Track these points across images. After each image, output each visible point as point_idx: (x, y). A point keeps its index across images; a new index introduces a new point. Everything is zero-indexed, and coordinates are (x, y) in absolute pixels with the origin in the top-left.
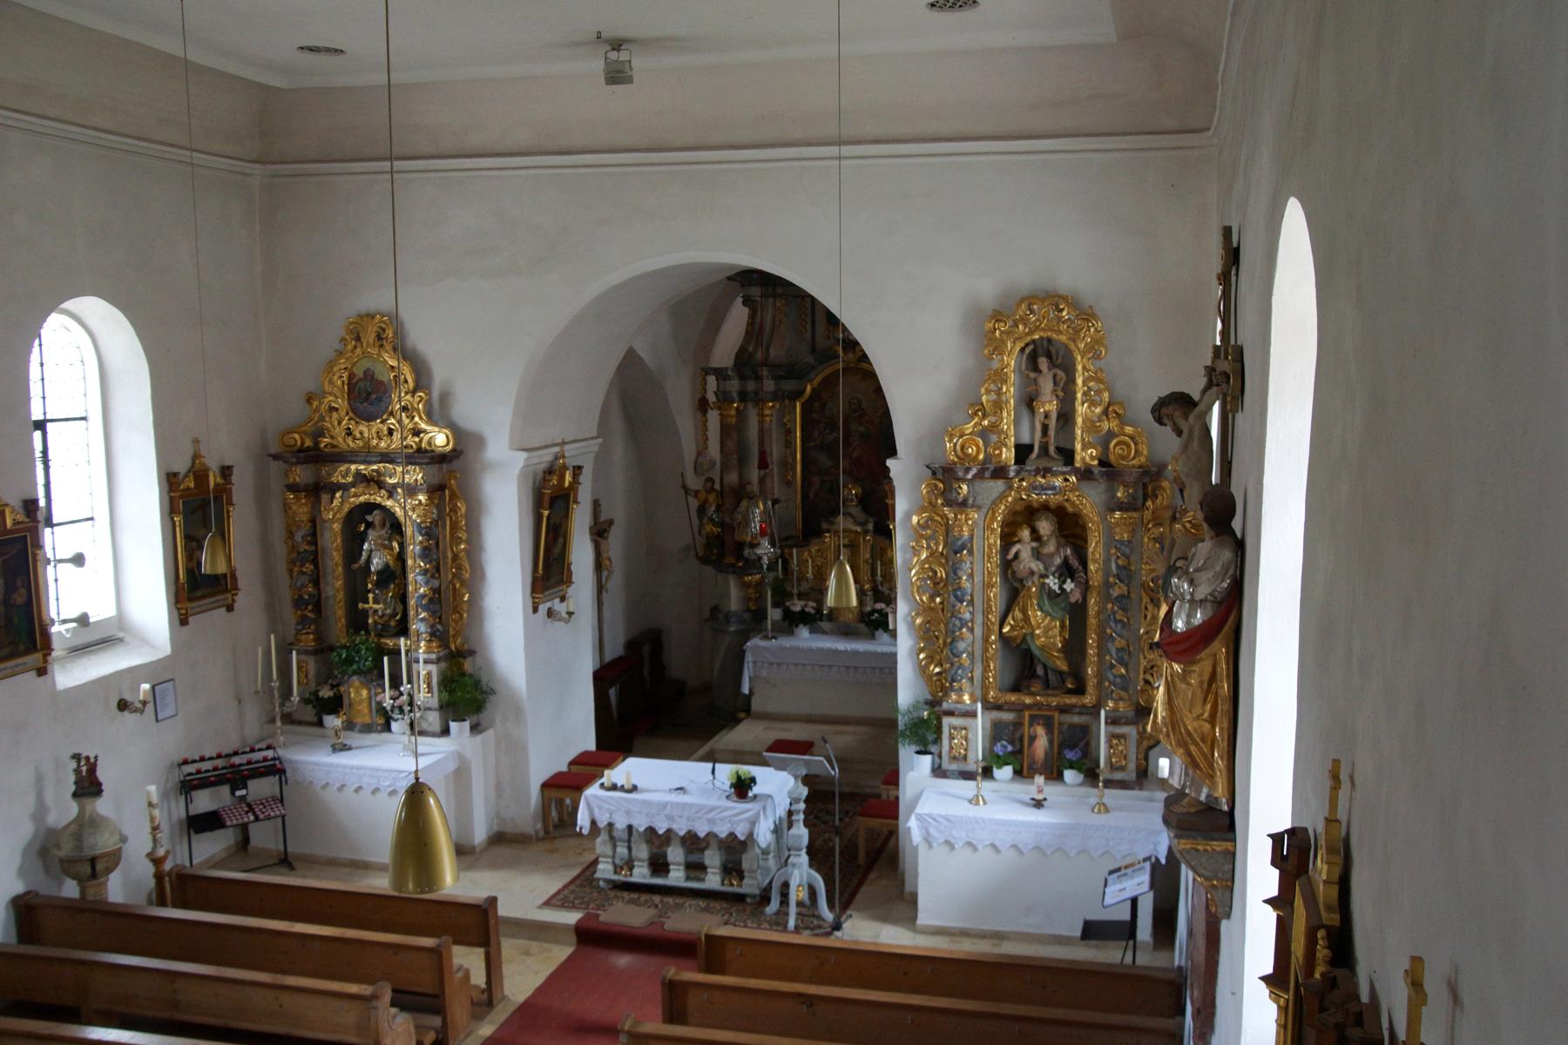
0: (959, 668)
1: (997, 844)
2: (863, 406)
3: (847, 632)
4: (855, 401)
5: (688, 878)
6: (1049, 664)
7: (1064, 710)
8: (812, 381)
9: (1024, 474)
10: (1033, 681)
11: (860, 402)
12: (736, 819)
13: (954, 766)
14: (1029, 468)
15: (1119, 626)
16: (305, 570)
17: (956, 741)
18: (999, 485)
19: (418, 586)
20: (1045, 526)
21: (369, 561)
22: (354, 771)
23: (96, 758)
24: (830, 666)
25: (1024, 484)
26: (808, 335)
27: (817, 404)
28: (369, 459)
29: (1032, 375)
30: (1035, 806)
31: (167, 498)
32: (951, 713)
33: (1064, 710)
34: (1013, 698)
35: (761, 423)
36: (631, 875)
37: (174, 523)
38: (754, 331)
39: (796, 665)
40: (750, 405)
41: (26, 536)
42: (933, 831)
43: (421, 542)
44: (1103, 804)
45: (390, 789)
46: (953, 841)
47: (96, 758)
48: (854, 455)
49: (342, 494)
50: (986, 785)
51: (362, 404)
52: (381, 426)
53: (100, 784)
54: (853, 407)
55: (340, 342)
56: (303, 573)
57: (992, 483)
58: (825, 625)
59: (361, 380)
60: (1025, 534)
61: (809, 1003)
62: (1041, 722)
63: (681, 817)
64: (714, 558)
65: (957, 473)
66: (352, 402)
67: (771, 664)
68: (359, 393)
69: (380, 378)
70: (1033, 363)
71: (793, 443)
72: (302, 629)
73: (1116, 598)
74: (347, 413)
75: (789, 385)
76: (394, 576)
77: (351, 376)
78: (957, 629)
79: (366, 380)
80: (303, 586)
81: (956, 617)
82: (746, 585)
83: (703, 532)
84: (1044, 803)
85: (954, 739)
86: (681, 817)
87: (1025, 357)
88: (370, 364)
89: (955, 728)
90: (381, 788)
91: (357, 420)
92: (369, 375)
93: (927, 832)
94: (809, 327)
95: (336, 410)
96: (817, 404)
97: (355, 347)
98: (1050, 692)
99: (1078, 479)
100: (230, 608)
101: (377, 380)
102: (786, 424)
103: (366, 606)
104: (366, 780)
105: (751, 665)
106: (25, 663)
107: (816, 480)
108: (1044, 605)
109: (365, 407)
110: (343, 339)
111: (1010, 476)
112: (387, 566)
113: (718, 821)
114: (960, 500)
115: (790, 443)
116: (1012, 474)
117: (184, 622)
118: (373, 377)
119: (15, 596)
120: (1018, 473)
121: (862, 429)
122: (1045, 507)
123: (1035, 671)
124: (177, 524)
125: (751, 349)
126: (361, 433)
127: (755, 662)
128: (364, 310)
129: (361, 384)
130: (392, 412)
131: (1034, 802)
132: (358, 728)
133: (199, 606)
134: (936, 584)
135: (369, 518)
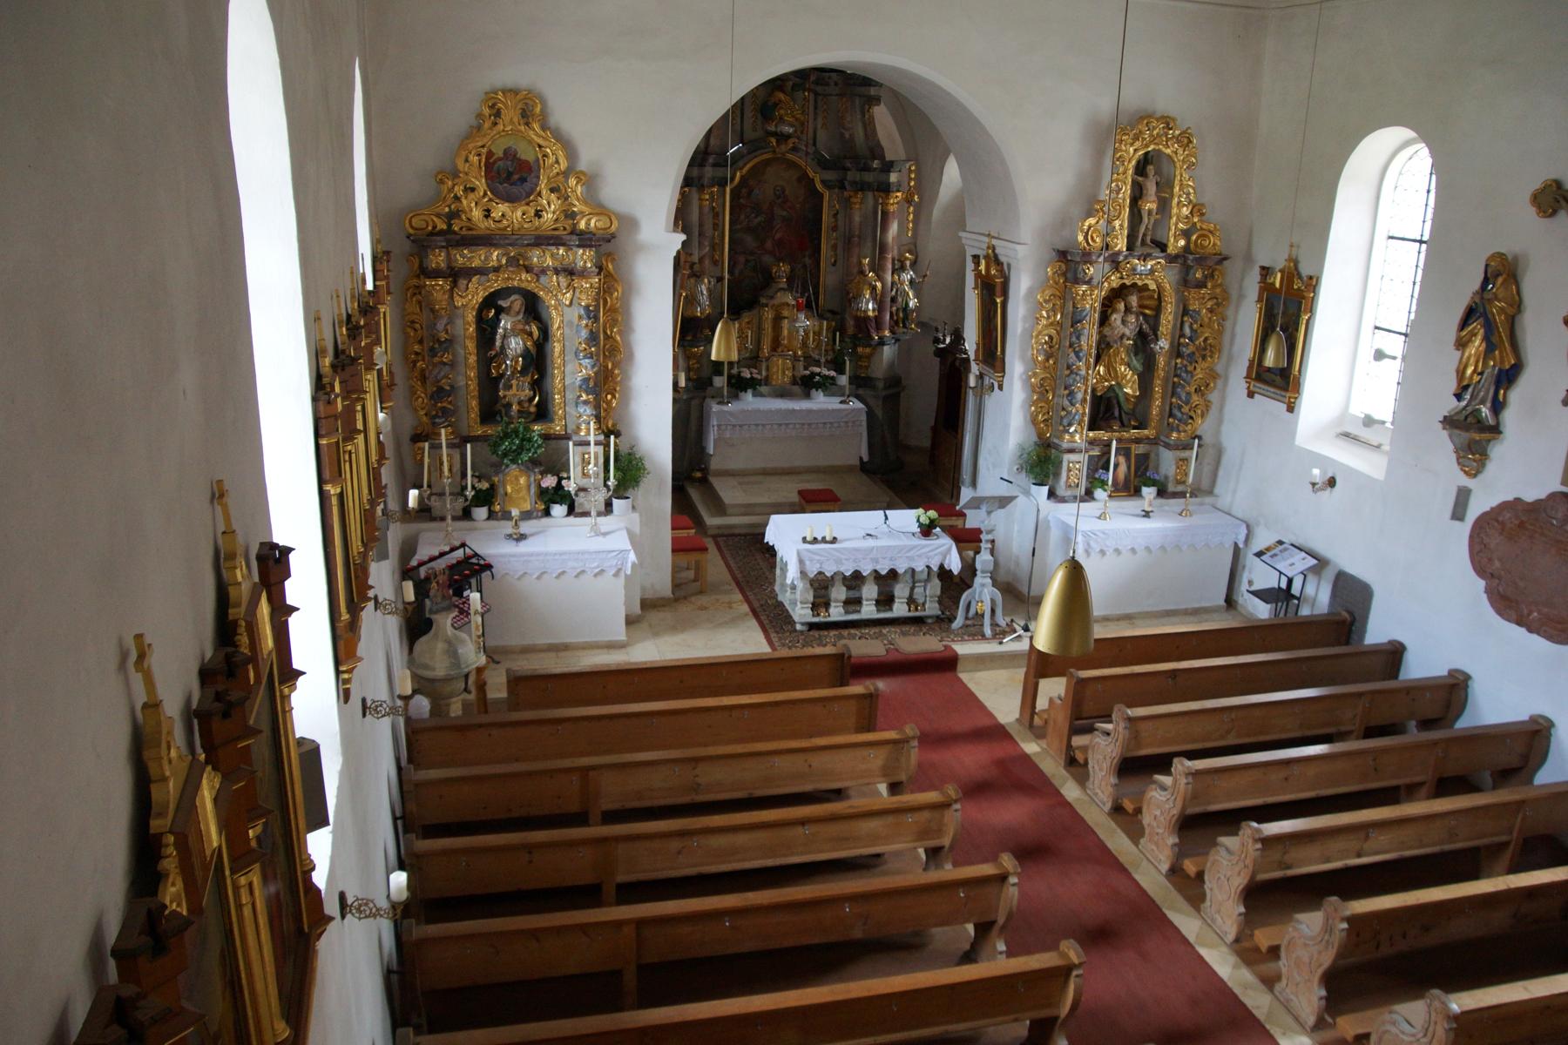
1: (1136, 547)
2: (787, 192)
3: (782, 394)
4: (778, 188)
5: (847, 612)
7: (1138, 441)
8: (741, 169)
10: (1112, 421)
12: (931, 554)
13: (1068, 493)
15: (1189, 375)
16: (445, 360)
21: (503, 347)
22: (556, 557)
24: (787, 424)
25: (1128, 265)
27: (744, 190)
29: (1140, 179)
30: (1144, 516)
32: (1071, 451)
35: (701, 207)
36: (829, 615)
39: (757, 425)
40: (694, 189)
42: (1092, 543)
45: (597, 570)
46: (1105, 549)
48: (778, 236)
49: (479, 279)
51: (501, 184)
52: (525, 208)
56: (445, 364)
58: (763, 389)
59: (500, 159)
60: (1121, 306)
63: (884, 558)
66: (489, 181)
67: (734, 426)
68: (498, 173)
69: (523, 157)
70: (1141, 169)
71: (720, 224)
72: (444, 422)
73: (1189, 355)
76: (537, 361)
77: (490, 154)
81: (1077, 374)
84: (1151, 514)
85: (1070, 471)
86: (884, 558)
88: (512, 143)
90: (587, 570)
92: (509, 154)
93: (1088, 544)
95: (473, 190)
96: (744, 190)
97: (495, 124)
101: (520, 160)
102: (714, 208)
104: (571, 564)
105: (716, 428)
107: (742, 259)
108: (1132, 361)
112: (526, 350)
113: (916, 558)
116: (1121, 258)
118: (515, 156)
120: (1126, 257)
121: (785, 213)
123: (1113, 414)
127: (719, 426)
129: (500, 163)
131: (1144, 513)
133: (1274, 393)
134: (1051, 347)
135: (504, 303)
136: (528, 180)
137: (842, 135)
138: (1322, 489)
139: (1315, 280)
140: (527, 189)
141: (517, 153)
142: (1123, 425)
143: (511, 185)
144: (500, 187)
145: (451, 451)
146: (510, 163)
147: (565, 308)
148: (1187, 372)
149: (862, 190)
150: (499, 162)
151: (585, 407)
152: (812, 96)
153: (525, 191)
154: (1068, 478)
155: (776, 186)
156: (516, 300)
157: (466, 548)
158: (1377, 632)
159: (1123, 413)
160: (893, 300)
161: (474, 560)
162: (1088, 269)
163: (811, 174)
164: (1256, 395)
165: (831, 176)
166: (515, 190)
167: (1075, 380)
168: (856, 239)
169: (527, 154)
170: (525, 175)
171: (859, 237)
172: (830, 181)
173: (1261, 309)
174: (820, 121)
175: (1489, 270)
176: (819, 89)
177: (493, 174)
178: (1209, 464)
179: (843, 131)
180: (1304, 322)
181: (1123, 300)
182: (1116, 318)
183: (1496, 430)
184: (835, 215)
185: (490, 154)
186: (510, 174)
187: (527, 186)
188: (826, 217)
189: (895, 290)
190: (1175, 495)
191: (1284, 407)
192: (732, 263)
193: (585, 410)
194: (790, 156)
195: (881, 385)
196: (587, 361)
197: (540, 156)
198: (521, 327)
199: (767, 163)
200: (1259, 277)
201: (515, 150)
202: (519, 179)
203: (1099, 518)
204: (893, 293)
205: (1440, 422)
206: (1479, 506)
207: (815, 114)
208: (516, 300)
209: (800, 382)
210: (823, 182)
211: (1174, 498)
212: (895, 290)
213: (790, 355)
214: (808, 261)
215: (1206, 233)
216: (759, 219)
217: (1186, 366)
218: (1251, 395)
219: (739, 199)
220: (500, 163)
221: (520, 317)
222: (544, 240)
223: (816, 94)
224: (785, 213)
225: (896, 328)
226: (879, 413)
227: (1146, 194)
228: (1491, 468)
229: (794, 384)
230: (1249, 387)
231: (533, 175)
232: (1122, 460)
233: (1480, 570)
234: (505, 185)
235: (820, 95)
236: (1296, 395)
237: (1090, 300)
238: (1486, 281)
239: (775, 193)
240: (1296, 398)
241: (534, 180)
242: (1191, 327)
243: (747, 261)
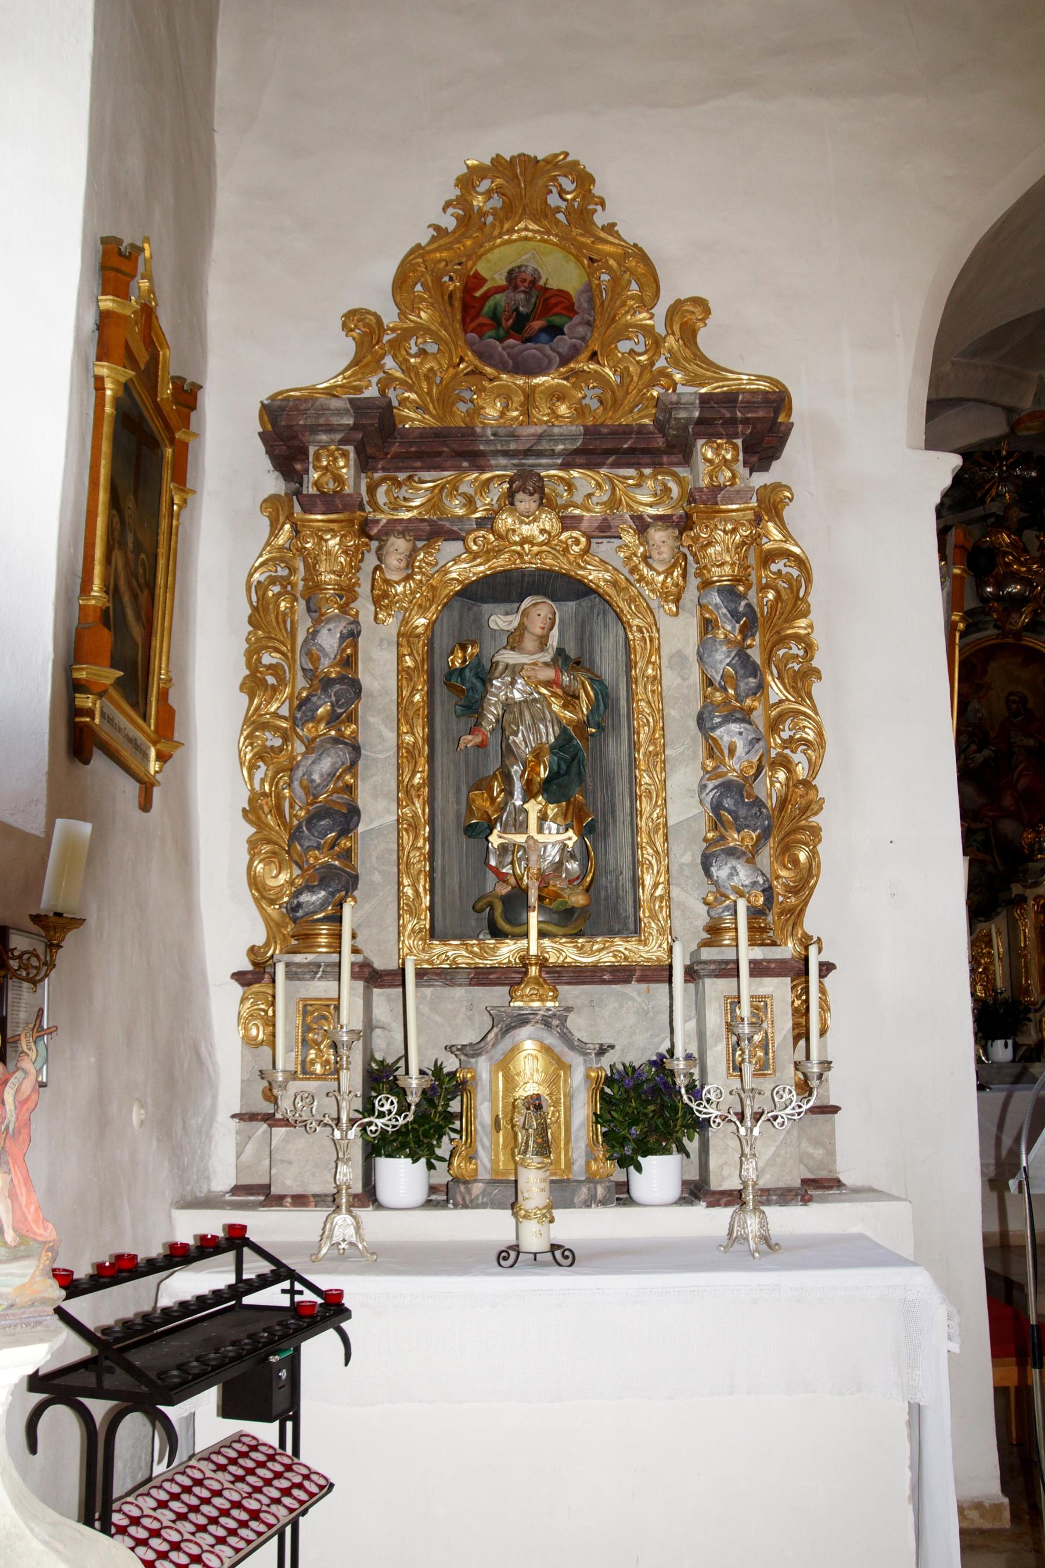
2: (1030, 705)
4: (1016, 698)
11: (1023, 700)
48: (1022, 784)
51: (501, 340)
54: (1014, 706)
55: (444, 210)
59: (499, 290)
69: (553, 285)
79: (515, 288)
91: (489, 370)
101: (545, 289)
109: (513, 347)
110: (448, 205)
118: (534, 282)
121: (1031, 742)
136: (566, 330)
140: (564, 349)
141: (540, 277)
146: (522, 296)
150: (498, 297)
151: (733, 862)
153: (559, 354)
155: (1011, 694)
166: (532, 350)
170: (557, 320)
177: (481, 320)
186: (520, 322)
187: (563, 343)
193: (734, 872)
196: (735, 727)
198: (550, 674)
202: (542, 330)
216: (986, 753)
221: (547, 657)
224: (1031, 742)
231: (577, 319)
234: (511, 341)
241: (581, 330)
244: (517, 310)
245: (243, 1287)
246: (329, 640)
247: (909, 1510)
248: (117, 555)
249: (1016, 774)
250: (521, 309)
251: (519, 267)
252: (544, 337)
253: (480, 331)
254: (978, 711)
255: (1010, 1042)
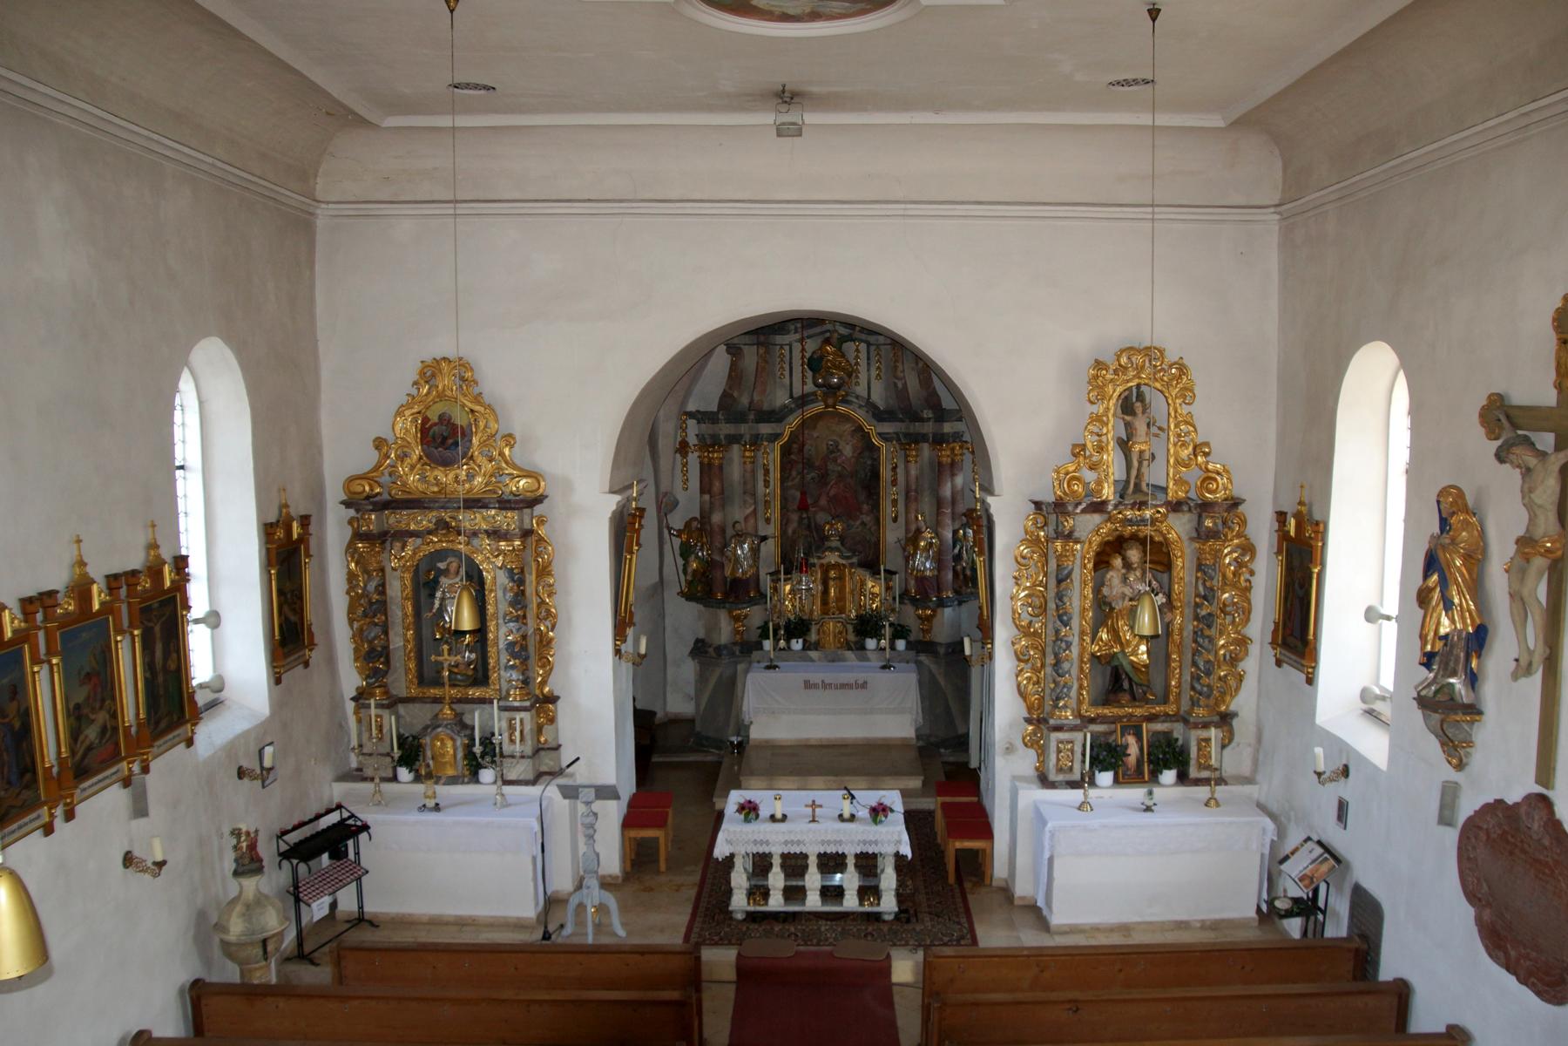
0: (1064, 687)
6: (1135, 679)
9: (1121, 507)
10: (1121, 695)
13: (1060, 777)
14: (1126, 502)
15: (1206, 641)
16: (376, 621)
17: (1062, 754)
18: (1096, 518)
19: (502, 634)
20: (1134, 555)
23: (257, 831)
26: (787, 381)
27: (795, 446)
28: (448, 505)
29: (1128, 418)
31: (264, 551)
32: (1058, 729)
33: (1152, 718)
34: (1106, 711)
37: (270, 574)
38: (735, 375)
41: (175, 597)
43: (512, 589)
44: (1215, 799)
47: (257, 831)
48: (832, 493)
50: (1092, 793)
51: (436, 448)
53: (261, 860)
55: (413, 386)
56: (376, 624)
57: (1088, 517)
59: (435, 424)
60: (1118, 562)
61: (1074, 1009)
62: (1132, 732)
64: (699, 594)
65: (1067, 508)
74: (421, 458)
75: (766, 429)
77: (426, 420)
78: (1062, 651)
79: (442, 424)
80: (375, 638)
82: (737, 619)
83: (690, 570)
85: (1061, 752)
87: (1120, 401)
88: (446, 408)
89: (1062, 742)
91: (432, 465)
92: (445, 420)
94: (787, 373)
96: (795, 446)
98: (1137, 704)
99: (1167, 510)
100: (306, 664)
103: (440, 658)
106: (178, 735)
109: (440, 451)
110: (415, 383)
111: (1109, 510)
114: (1066, 533)
115: (769, 481)
116: (1110, 508)
117: (278, 681)
118: (449, 420)
119: (170, 662)
120: (1116, 506)
122: (1134, 537)
124: (273, 577)
125: (736, 394)
126: (436, 478)
128: (438, 356)
129: (436, 428)
130: (472, 456)
132: (442, 781)
135: (442, 566)
137: (895, 385)
138: (1331, 780)
139: (1321, 526)
142: (1134, 698)
143: (446, 449)
144: (435, 451)
145: (380, 711)
146: (444, 428)
147: (498, 570)
148: (1203, 636)
149: (917, 442)
150: (435, 428)
152: (863, 347)
154: (1058, 760)
156: (451, 562)
157: (343, 810)
158: (1388, 970)
159: (1133, 684)
160: (958, 558)
161: (351, 822)
162: (1067, 521)
163: (867, 428)
164: (1285, 665)
165: (888, 428)
166: (448, 453)
167: (1060, 648)
168: (913, 493)
169: (460, 419)
171: (916, 491)
172: (888, 433)
173: (1282, 561)
174: (874, 373)
175: (1442, 507)
176: (872, 339)
177: (429, 439)
178: (1250, 745)
179: (896, 381)
180: (1315, 576)
181: (1120, 554)
182: (1114, 576)
183: (1474, 710)
184: (894, 469)
185: (426, 420)
186: (445, 439)
188: (885, 473)
189: (958, 547)
190: (1198, 782)
191: (1303, 677)
192: (785, 521)
193: (511, 675)
194: (841, 408)
195: (942, 651)
196: (512, 624)
197: (472, 420)
199: (818, 417)
200: (1277, 524)
201: (450, 415)
202: (452, 444)
203: (1207, 804)
204: (956, 551)
205: (1414, 699)
206: (1468, 807)
207: (868, 364)
208: (451, 562)
209: (854, 648)
210: (880, 434)
211: (1197, 785)
212: (958, 547)
213: (842, 618)
214: (867, 519)
215: (1214, 475)
217: (1202, 630)
218: (1279, 663)
219: (789, 455)
220: (436, 428)
222: (473, 504)
223: (869, 344)
225: (964, 588)
226: (941, 680)
227: (1136, 435)
228: (1477, 758)
229: (848, 650)
230: (1275, 655)
232: (1131, 740)
233: (1471, 896)
234: (440, 449)
235: (872, 345)
236: (1313, 665)
237: (1081, 555)
238: (1444, 522)
239: (828, 448)
240: (1314, 668)
242: (1204, 584)
243: (801, 519)
244: (442, 435)
245: (343, 821)
246: (372, 586)
247: (532, 884)
248: (286, 609)
249: (829, 487)
250: (444, 434)
251: (443, 413)
252: (453, 447)
253: (428, 444)
254: (810, 450)
255: (800, 641)
